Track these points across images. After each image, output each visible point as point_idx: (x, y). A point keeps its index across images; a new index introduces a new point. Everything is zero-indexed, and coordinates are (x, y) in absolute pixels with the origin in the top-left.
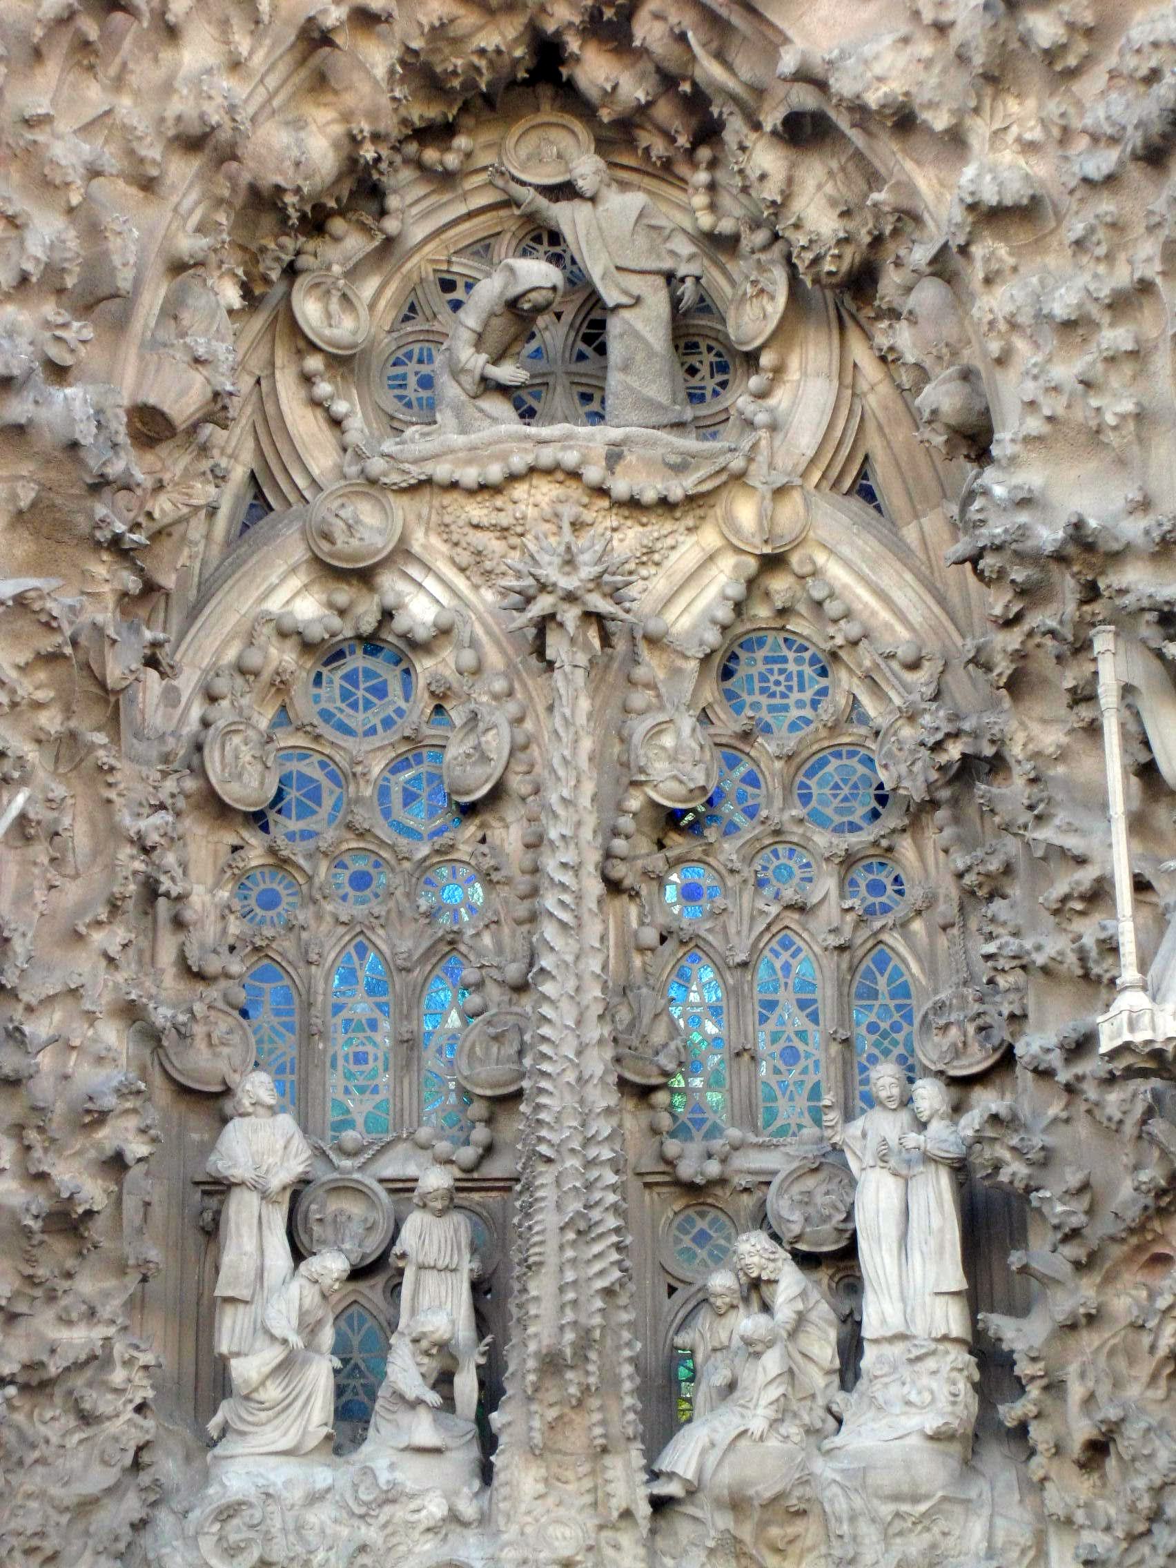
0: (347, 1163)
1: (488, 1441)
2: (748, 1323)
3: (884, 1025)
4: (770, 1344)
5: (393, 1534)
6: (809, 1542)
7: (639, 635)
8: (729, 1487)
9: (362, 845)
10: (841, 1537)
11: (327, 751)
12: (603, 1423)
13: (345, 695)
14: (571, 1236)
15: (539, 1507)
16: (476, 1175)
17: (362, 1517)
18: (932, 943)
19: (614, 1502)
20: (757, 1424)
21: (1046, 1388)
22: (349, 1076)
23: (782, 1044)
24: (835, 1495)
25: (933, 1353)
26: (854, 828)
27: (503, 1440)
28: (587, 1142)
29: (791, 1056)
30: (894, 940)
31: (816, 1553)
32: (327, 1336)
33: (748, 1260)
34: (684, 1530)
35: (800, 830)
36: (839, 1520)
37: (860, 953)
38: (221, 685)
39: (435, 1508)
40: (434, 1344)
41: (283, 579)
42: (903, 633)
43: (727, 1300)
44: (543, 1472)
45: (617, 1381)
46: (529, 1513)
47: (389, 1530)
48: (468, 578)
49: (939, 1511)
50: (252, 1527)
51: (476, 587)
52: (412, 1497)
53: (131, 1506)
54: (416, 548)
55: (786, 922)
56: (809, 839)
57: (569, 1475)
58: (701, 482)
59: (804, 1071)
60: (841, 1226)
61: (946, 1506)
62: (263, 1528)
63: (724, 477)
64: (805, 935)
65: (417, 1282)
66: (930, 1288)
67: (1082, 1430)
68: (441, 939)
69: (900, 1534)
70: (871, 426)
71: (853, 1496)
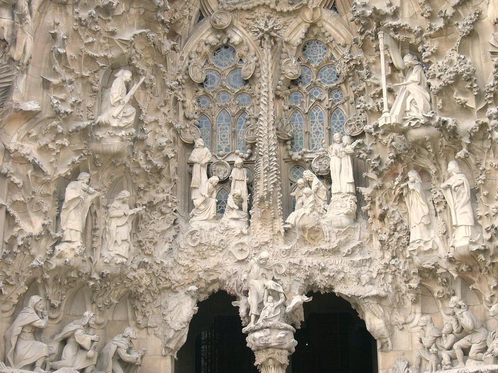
0: (220, 158)
1: (250, 216)
2: (307, 190)
3: (338, 126)
4: (310, 195)
18: (349, 107)
20: (308, 211)
21: (371, 203)
22: (221, 140)
23: (316, 130)
25: (347, 196)
26: (332, 83)
28: (270, 151)
29: (317, 133)
30: (341, 107)
32: (215, 195)
37: (333, 110)
38: (193, 56)
39: (238, 232)
40: (237, 196)
41: (206, 32)
42: (342, 39)
45: (276, 203)
49: (349, 230)
51: (248, 32)
53: (173, 232)
54: (235, 24)
58: (297, 7)
59: (321, 136)
62: (200, 236)
63: (302, 6)
65: (235, 183)
67: (379, 211)
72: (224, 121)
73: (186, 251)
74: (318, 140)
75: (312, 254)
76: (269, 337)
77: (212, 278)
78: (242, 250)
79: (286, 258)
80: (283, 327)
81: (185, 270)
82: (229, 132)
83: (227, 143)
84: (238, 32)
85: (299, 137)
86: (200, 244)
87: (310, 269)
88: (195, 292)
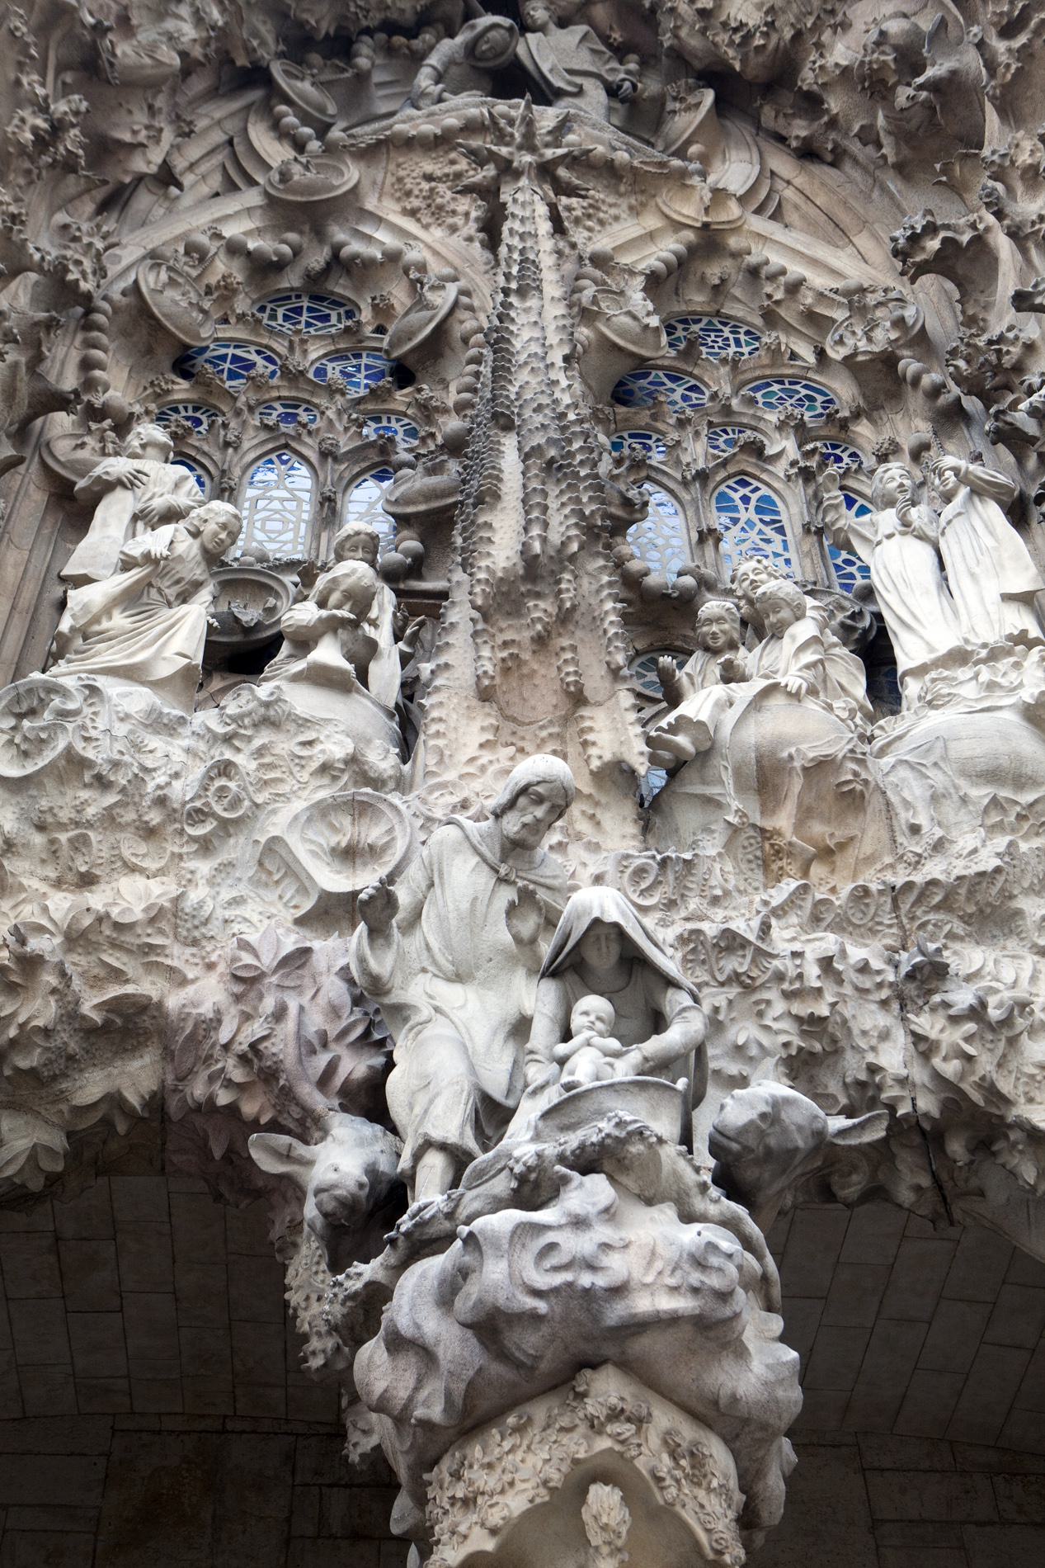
5: (271, 766)
8: (757, 748)
9: (293, 394)
10: (915, 830)
11: (265, 341)
13: (286, 318)
14: (536, 463)
15: (486, 757)
17: (228, 739)
19: (593, 751)
24: (903, 780)
25: (1009, 653)
31: (878, 866)
33: (752, 577)
34: (687, 818)
35: (751, 412)
39: (336, 748)
43: (726, 626)
46: (472, 760)
48: (418, 220)
50: (64, 714)
51: (426, 227)
52: (304, 723)
56: (761, 419)
60: (849, 622)
64: (764, 476)
75: (829, 918)
76: (602, 1232)
77: (114, 991)
84: (382, 235)
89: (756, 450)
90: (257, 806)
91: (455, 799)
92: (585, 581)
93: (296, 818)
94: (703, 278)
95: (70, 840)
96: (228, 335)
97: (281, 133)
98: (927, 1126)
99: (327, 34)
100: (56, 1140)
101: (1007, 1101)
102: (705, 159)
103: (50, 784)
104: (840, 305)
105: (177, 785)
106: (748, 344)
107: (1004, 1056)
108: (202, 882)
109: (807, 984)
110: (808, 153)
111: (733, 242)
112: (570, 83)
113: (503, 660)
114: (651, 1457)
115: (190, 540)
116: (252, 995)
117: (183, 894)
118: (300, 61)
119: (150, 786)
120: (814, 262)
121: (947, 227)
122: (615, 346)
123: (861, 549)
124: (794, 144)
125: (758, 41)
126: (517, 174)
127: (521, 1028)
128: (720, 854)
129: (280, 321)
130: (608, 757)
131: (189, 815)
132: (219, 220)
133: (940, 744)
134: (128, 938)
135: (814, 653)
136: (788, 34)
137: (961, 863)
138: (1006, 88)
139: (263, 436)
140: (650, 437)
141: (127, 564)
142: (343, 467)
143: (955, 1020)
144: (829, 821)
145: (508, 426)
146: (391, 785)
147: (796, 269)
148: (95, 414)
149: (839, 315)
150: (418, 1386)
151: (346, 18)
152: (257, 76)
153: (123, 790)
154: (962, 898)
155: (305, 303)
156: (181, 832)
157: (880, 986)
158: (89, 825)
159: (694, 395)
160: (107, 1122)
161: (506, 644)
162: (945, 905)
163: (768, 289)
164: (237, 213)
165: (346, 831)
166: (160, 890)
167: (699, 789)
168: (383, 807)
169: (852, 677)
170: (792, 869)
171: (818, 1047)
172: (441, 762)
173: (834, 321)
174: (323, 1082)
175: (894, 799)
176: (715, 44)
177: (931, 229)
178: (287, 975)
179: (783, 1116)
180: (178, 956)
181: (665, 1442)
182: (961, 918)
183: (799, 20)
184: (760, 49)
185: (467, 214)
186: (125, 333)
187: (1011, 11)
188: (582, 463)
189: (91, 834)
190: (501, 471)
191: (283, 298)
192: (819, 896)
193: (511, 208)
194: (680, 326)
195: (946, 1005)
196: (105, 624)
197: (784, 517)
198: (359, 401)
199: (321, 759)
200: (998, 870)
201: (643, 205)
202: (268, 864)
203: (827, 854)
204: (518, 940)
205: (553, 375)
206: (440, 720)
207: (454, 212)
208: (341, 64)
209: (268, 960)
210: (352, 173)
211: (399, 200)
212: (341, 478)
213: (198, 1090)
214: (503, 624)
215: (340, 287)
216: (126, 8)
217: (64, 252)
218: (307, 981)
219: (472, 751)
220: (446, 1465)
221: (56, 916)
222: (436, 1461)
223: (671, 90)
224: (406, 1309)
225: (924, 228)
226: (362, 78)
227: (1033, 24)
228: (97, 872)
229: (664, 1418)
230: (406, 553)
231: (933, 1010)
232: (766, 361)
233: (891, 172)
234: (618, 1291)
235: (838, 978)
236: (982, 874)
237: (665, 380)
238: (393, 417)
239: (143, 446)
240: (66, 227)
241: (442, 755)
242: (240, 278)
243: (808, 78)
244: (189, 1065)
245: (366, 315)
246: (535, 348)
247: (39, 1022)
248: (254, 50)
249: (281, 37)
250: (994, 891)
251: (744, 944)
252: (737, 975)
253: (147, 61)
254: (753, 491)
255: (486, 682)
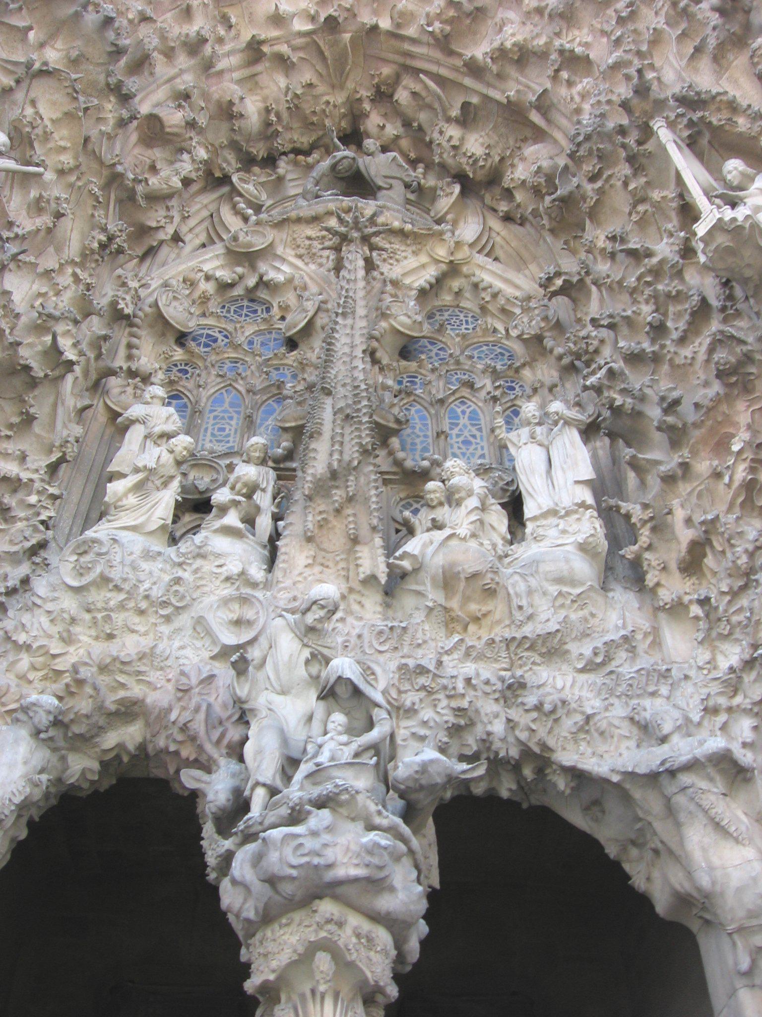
1: (275, 537)
5: (201, 578)
6: (497, 616)
7: (388, 280)
8: (443, 567)
10: (520, 608)
11: (223, 326)
12: (356, 523)
14: (340, 416)
15: (308, 571)
16: (282, 466)
17: (180, 565)
19: (361, 569)
20: (463, 531)
22: (213, 435)
24: (517, 582)
25: (576, 512)
27: (285, 533)
31: (503, 625)
33: (452, 470)
34: (408, 602)
36: (517, 595)
39: (234, 568)
40: (245, 485)
43: (438, 495)
44: (312, 553)
45: (367, 499)
46: (301, 574)
47: (198, 576)
49: (588, 597)
50: (99, 554)
51: (307, 264)
52: (218, 556)
55: (464, 394)
57: (331, 564)
59: (476, 449)
60: (505, 487)
61: (592, 594)
64: (474, 399)
66: (570, 482)
67: (686, 536)
68: (273, 385)
69: (562, 606)
70: (497, 247)
71: (530, 579)
72: (226, 405)
73: (50, 606)
74: (468, 455)
75: (474, 654)
76: (326, 838)
77: (122, 694)
78: (238, 623)
79: (388, 655)
80: (385, 822)
81: (34, 668)
82: (237, 424)
83: (228, 442)
84: (285, 268)
85: (419, 447)
86: (104, 580)
87: (472, 693)
88: (49, 712)
89: (470, 385)
90: (194, 600)
91: (290, 595)
92: (362, 480)
93: (211, 606)
94: (450, 288)
95: (102, 617)
96: (205, 323)
97: (237, 212)
98: (513, 762)
99: (263, 157)
100: (96, 766)
101: (551, 750)
102: (455, 223)
103: (93, 590)
104: (517, 306)
105: (155, 587)
106: (472, 323)
107: (552, 728)
108: (165, 638)
109: (458, 691)
110: (507, 218)
111: (465, 269)
112: (386, 183)
113: (319, 521)
114: (346, 938)
115: (169, 455)
116: (186, 697)
117: (155, 646)
118: (248, 171)
119: (142, 589)
120: (506, 281)
121: (566, 273)
122: (399, 332)
123: (512, 450)
124: (501, 214)
125: (481, 163)
126: (351, 241)
127: (310, 718)
128: (423, 621)
129: (232, 313)
130: (368, 572)
131: (160, 604)
132: (201, 262)
133: (535, 564)
134: (127, 668)
135: (476, 515)
136: (497, 159)
137: (540, 626)
138: (591, 208)
139: (219, 380)
140: (416, 377)
141: (137, 470)
142: (258, 397)
143: (527, 711)
144: (479, 603)
145: (329, 393)
146: (261, 586)
147: (498, 284)
148: (132, 374)
149: (518, 311)
150: (245, 900)
151: (272, 149)
152: (226, 180)
153: (128, 592)
154: (539, 645)
155: (246, 303)
156: (157, 612)
157: (495, 691)
158: (112, 610)
159: (441, 353)
160: (118, 757)
161: (320, 513)
162: (531, 648)
163: (483, 295)
164: (211, 258)
165: (236, 611)
166: (146, 643)
167: (414, 587)
168: (254, 600)
169: (499, 520)
170: (459, 628)
171: (462, 722)
172: (284, 576)
173: (515, 314)
174: (218, 742)
175: (511, 591)
176: (460, 163)
177: (558, 274)
178: (203, 688)
179: (429, 769)
180: (154, 676)
181: (354, 932)
182: (539, 654)
183: (503, 152)
184: (482, 167)
185: (328, 257)
186: (151, 326)
187: (594, 169)
188: (365, 414)
189: (112, 614)
190: (323, 419)
191: (234, 300)
192: (470, 644)
193: (346, 264)
194: (438, 314)
195: (523, 704)
196: (125, 502)
197: (482, 422)
198: (269, 360)
199: (225, 574)
200: (558, 631)
201: (420, 250)
202: (199, 629)
203: (477, 620)
204: (311, 676)
205: (355, 363)
206: (286, 554)
207: (321, 256)
208: (270, 172)
209: (194, 681)
210: (271, 235)
211: (294, 249)
212: (256, 403)
213: (161, 743)
214: (319, 502)
215: (263, 294)
216: (154, 161)
217: (117, 293)
218: (213, 691)
219: (300, 569)
220: (259, 936)
221: (94, 657)
222: (254, 935)
223: (440, 184)
224: (238, 868)
225: (555, 273)
226: (280, 179)
227: (605, 176)
228: (115, 632)
229: (354, 920)
230: (284, 449)
231: (517, 706)
232: (480, 333)
233: (548, 233)
234: (330, 866)
235: (474, 688)
236: (549, 633)
237: (427, 344)
238: (286, 368)
239: (152, 398)
240: (119, 277)
241: (285, 572)
242: (212, 293)
243: (506, 183)
244: (157, 729)
245: (275, 311)
246: (347, 350)
247: (84, 712)
248: (224, 169)
249: (239, 160)
250: (556, 641)
251: (428, 671)
252: (425, 687)
253: (165, 186)
254: (468, 408)
255: (309, 534)
